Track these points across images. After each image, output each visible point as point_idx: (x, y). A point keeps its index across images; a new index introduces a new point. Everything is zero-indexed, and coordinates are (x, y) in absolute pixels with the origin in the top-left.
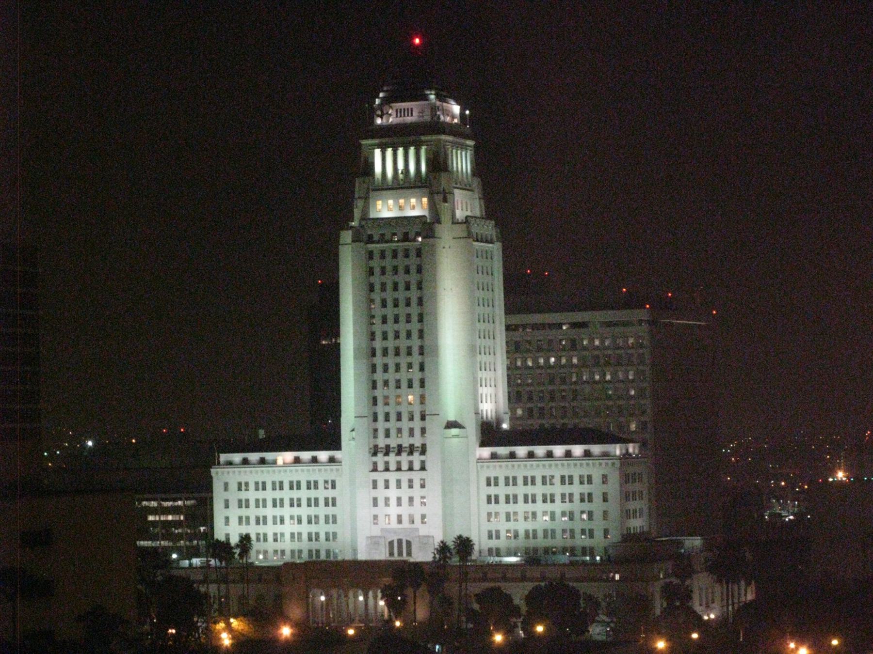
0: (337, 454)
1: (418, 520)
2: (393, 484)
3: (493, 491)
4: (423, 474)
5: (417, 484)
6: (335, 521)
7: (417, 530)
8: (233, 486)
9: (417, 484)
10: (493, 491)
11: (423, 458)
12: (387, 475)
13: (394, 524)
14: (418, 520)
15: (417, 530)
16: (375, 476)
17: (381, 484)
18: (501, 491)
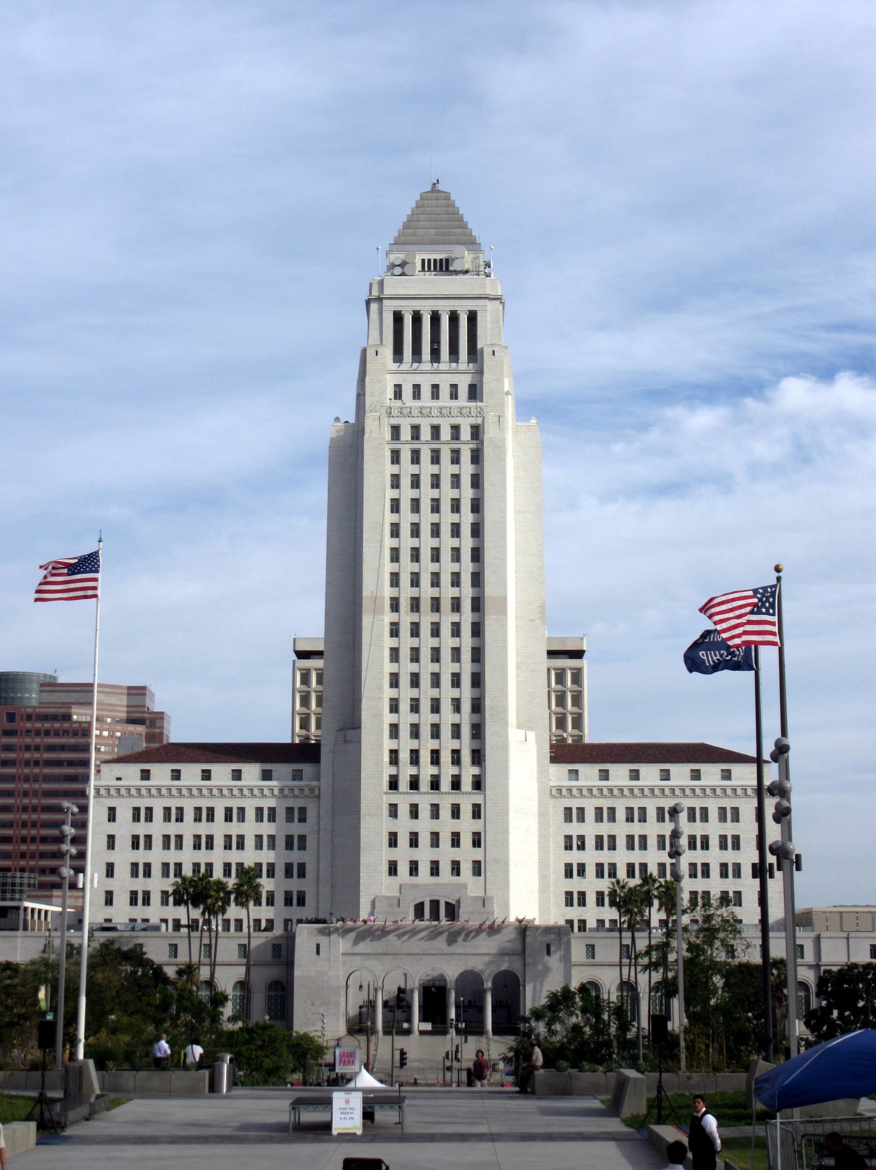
0: (307, 769)
1: (466, 868)
2: (425, 812)
3: (575, 829)
4: (478, 799)
5: (466, 811)
6: (302, 874)
7: (465, 886)
8: (124, 814)
9: (466, 811)
10: (575, 829)
11: (476, 770)
12: (415, 798)
14: (466, 868)
15: (465, 886)
16: (394, 798)
17: (404, 811)
18: (590, 829)
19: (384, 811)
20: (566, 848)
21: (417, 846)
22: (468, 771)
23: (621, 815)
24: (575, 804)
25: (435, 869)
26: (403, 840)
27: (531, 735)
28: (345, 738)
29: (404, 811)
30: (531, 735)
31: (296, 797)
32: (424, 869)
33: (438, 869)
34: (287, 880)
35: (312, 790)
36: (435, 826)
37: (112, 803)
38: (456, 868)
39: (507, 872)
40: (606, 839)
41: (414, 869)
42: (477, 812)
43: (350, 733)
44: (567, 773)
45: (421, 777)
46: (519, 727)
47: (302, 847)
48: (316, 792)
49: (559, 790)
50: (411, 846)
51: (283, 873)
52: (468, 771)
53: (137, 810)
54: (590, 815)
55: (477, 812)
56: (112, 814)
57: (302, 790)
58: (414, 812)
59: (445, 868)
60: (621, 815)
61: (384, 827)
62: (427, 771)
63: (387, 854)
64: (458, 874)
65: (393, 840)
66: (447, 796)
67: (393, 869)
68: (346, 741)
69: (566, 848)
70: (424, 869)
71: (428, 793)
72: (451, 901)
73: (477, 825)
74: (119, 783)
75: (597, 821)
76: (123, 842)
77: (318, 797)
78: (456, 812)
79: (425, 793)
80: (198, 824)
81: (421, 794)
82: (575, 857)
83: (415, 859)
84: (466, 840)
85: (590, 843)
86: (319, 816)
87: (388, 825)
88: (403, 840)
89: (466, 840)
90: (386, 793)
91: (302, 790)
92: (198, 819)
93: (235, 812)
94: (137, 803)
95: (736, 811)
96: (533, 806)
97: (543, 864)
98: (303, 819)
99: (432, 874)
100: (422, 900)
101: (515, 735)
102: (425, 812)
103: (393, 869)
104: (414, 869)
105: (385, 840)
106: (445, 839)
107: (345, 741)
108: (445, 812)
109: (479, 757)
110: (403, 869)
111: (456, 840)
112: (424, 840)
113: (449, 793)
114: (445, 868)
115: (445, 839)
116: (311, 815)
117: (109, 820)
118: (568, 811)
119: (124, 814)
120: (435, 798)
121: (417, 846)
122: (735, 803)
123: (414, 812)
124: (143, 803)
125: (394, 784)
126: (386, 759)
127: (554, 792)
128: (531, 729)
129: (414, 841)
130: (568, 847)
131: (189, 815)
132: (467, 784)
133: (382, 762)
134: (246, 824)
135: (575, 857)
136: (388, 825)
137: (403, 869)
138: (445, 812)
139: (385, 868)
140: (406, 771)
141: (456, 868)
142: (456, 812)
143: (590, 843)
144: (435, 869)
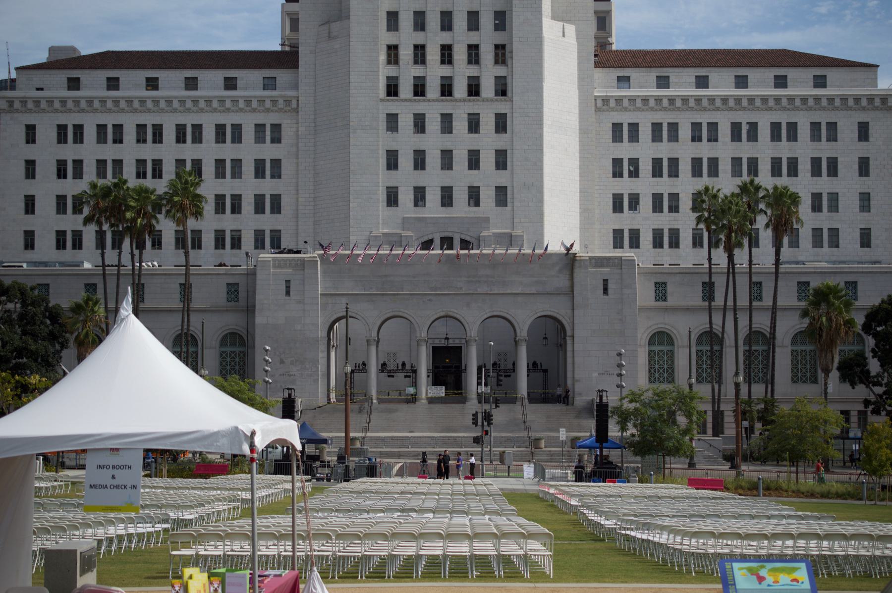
0: (282, 76)
1: (488, 196)
2: (433, 124)
4: (502, 107)
5: (488, 123)
6: (276, 205)
7: (487, 220)
8: (46, 133)
9: (488, 123)
10: (626, 150)
11: (501, 71)
12: (420, 106)
13: (433, 207)
14: (488, 196)
15: (487, 220)
16: (393, 106)
17: (406, 122)
19: (380, 123)
20: (614, 175)
21: (423, 168)
22: (488, 72)
23: (685, 132)
24: (625, 118)
25: (447, 197)
26: (406, 161)
27: (571, 29)
28: (329, 33)
29: (406, 122)
30: (571, 29)
31: (268, 110)
32: (433, 197)
33: (451, 197)
34: (257, 216)
35: (288, 102)
36: (446, 141)
37: (30, 119)
38: (474, 196)
39: (541, 201)
40: (665, 164)
41: (420, 196)
42: (501, 123)
43: (335, 27)
44: (616, 81)
45: (428, 80)
46: (555, 17)
47: (277, 174)
48: (294, 103)
49: (606, 100)
50: (416, 168)
51: (252, 208)
52: (488, 72)
53: (62, 130)
54: (645, 132)
55: (501, 123)
56: (31, 134)
57: (274, 102)
58: (420, 124)
59: (460, 196)
60: (685, 132)
61: (380, 144)
62: (434, 71)
63: (384, 178)
64: (477, 204)
65: (392, 161)
66: (463, 103)
67: (392, 198)
68: (330, 37)
69: (614, 175)
70: (433, 197)
71: (437, 100)
72: (468, 239)
73: (501, 142)
74: (40, 93)
75: (654, 140)
76: (46, 169)
77: (296, 110)
78: (474, 125)
79: (433, 100)
80: (142, 145)
81: (429, 100)
82: (626, 186)
83: (421, 185)
84: (488, 160)
85: (646, 168)
86: (297, 136)
87: (385, 141)
88: (406, 161)
89: (488, 160)
90: (382, 100)
91: (274, 102)
92: (141, 140)
93: (189, 130)
94: (63, 119)
95: (832, 127)
96: (573, 119)
97: (585, 194)
98: (276, 140)
99: (443, 205)
100: (430, 237)
101: (550, 28)
102: (433, 124)
103: (392, 198)
104: (420, 196)
105: (383, 161)
106: (460, 159)
107: (329, 37)
108: (460, 125)
109: (504, 55)
110: (406, 197)
111: (474, 161)
112: (433, 160)
113: (464, 100)
114: (460, 196)
115: (460, 159)
116: (287, 134)
117: (28, 142)
118: (617, 128)
119: (46, 133)
120: (446, 107)
121: (423, 168)
122: (832, 117)
123: (420, 124)
124: (71, 120)
125: (392, 89)
126: (383, 57)
127: (599, 103)
128: (569, 21)
129: (420, 161)
130: (617, 173)
131: (130, 134)
132: (488, 88)
133: (378, 60)
134: (203, 145)
135: (626, 186)
136: (385, 141)
137: (406, 197)
138: (460, 125)
139: (382, 196)
140: (408, 72)
141: (474, 196)
142: (474, 125)
143: (646, 168)
144: (447, 197)
